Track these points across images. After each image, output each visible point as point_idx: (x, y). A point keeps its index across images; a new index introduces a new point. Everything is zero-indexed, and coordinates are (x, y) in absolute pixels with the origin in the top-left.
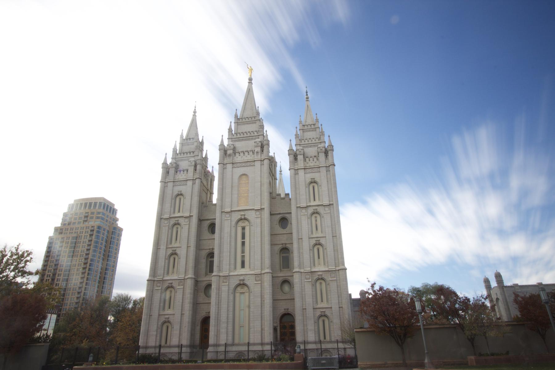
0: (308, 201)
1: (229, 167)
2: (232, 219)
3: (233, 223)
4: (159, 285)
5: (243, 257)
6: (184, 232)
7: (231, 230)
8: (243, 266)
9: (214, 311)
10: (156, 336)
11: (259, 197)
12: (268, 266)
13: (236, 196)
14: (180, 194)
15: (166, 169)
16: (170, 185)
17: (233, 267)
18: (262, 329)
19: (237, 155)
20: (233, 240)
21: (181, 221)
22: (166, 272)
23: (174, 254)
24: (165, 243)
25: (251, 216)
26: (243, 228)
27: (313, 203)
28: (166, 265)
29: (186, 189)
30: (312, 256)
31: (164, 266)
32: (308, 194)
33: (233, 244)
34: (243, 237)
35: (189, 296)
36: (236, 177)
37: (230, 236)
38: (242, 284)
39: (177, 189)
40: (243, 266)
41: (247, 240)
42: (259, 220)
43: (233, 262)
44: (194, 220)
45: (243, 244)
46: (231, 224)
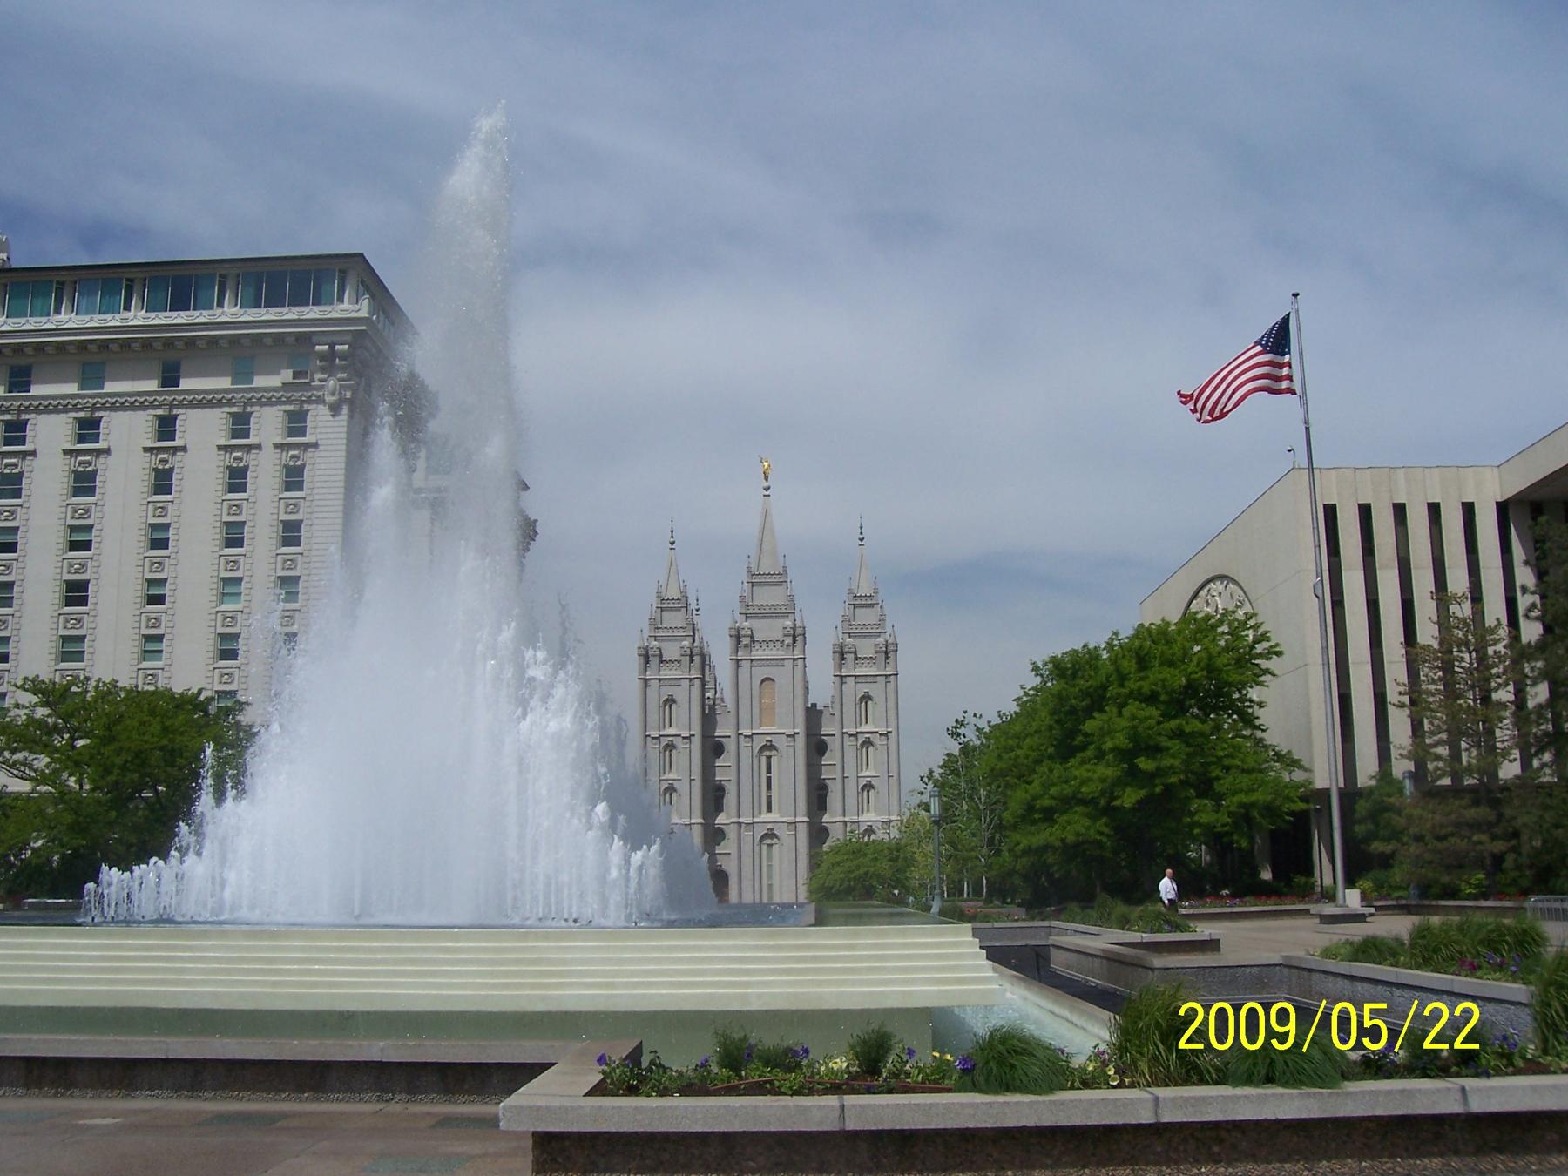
1: (746, 664)
3: (756, 751)
5: (769, 798)
8: (769, 810)
14: (670, 701)
15: (646, 657)
16: (654, 684)
19: (757, 646)
21: (677, 741)
23: (671, 789)
25: (780, 742)
26: (769, 758)
27: (864, 728)
29: (680, 693)
34: (769, 771)
36: (757, 682)
38: (770, 835)
39: (667, 692)
40: (769, 810)
41: (774, 775)
44: (697, 741)
45: (769, 779)
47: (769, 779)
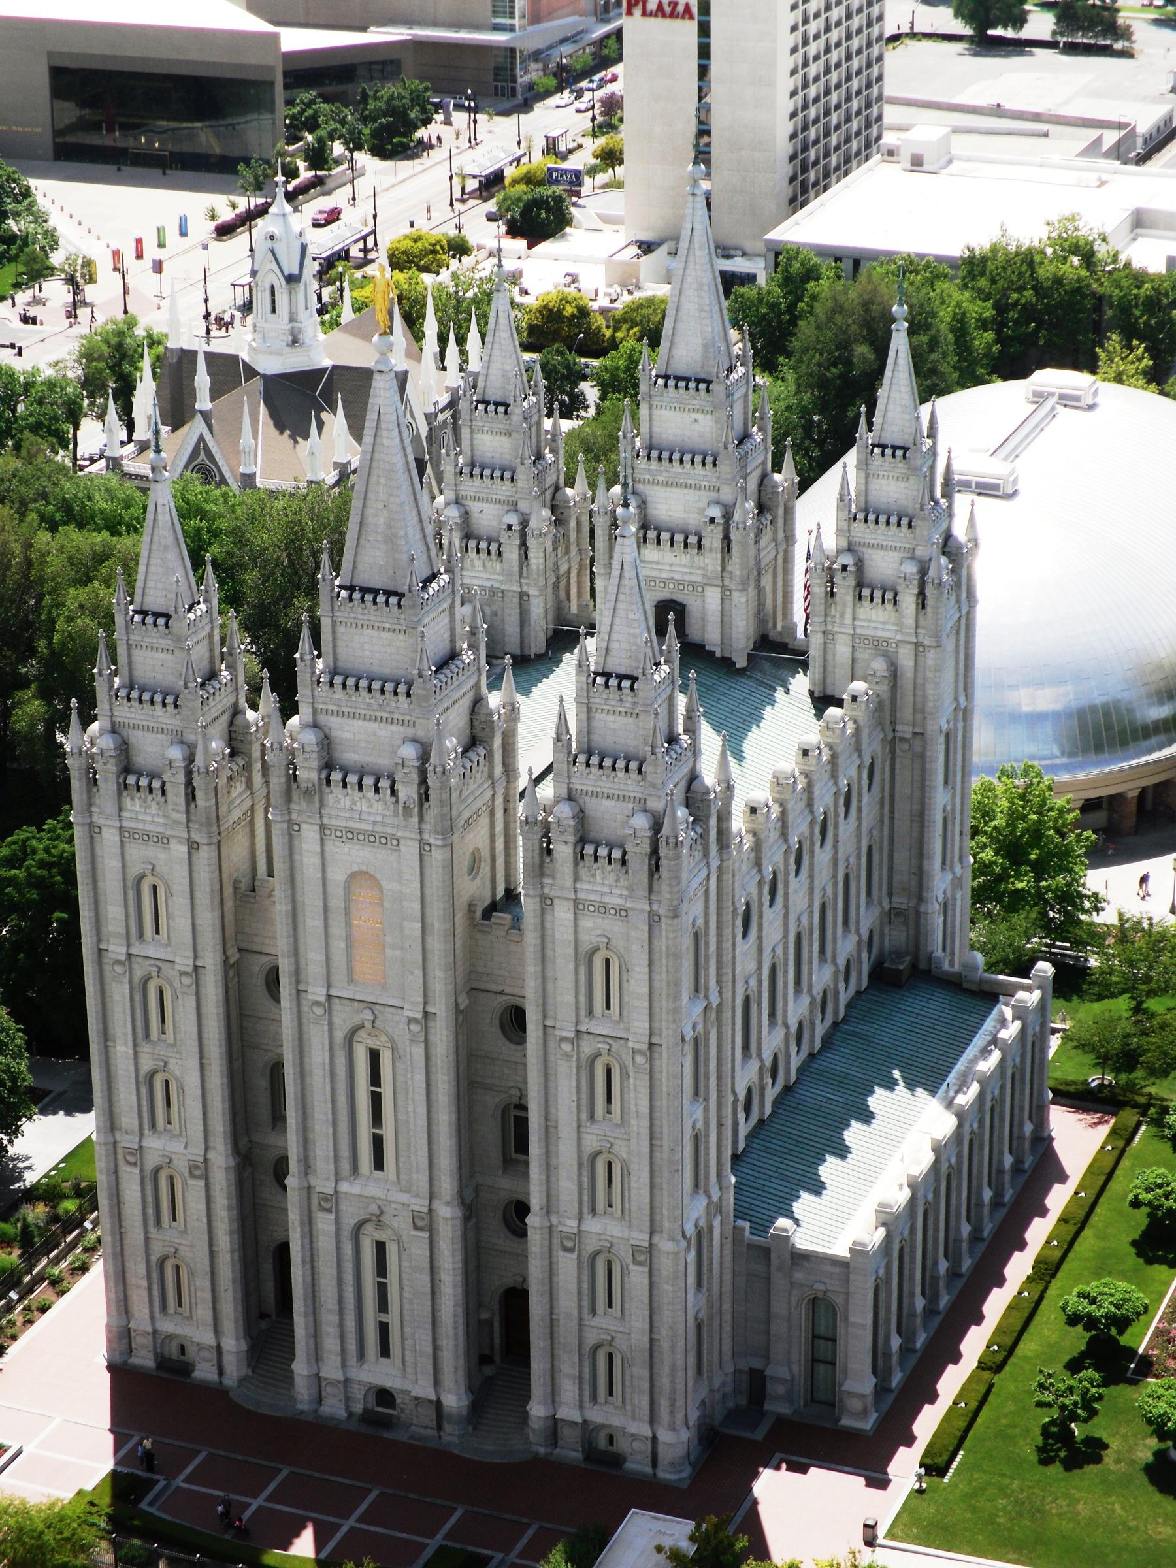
0: (583, 1013)
2: (337, 1020)
4: (131, 1159)
6: (183, 1013)
7: (332, 1057)
9: (300, 1279)
10: (150, 1289)
11: (418, 972)
12: (449, 1198)
13: (343, 945)
17: (346, 1166)
18: (436, 1348)
20: (342, 1086)
22: (146, 1121)
24: (130, 1037)
28: (145, 1103)
30: (586, 1185)
31: (139, 1105)
32: (583, 990)
33: (342, 1099)
34: (375, 1079)
35: (225, 1214)
36: (337, 875)
37: (332, 1074)
41: (386, 1090)
42: (419, 1050)
43: (345, 1152)
45: (376, 1099)
46: (331, 1037)
47: (376, 1099)
